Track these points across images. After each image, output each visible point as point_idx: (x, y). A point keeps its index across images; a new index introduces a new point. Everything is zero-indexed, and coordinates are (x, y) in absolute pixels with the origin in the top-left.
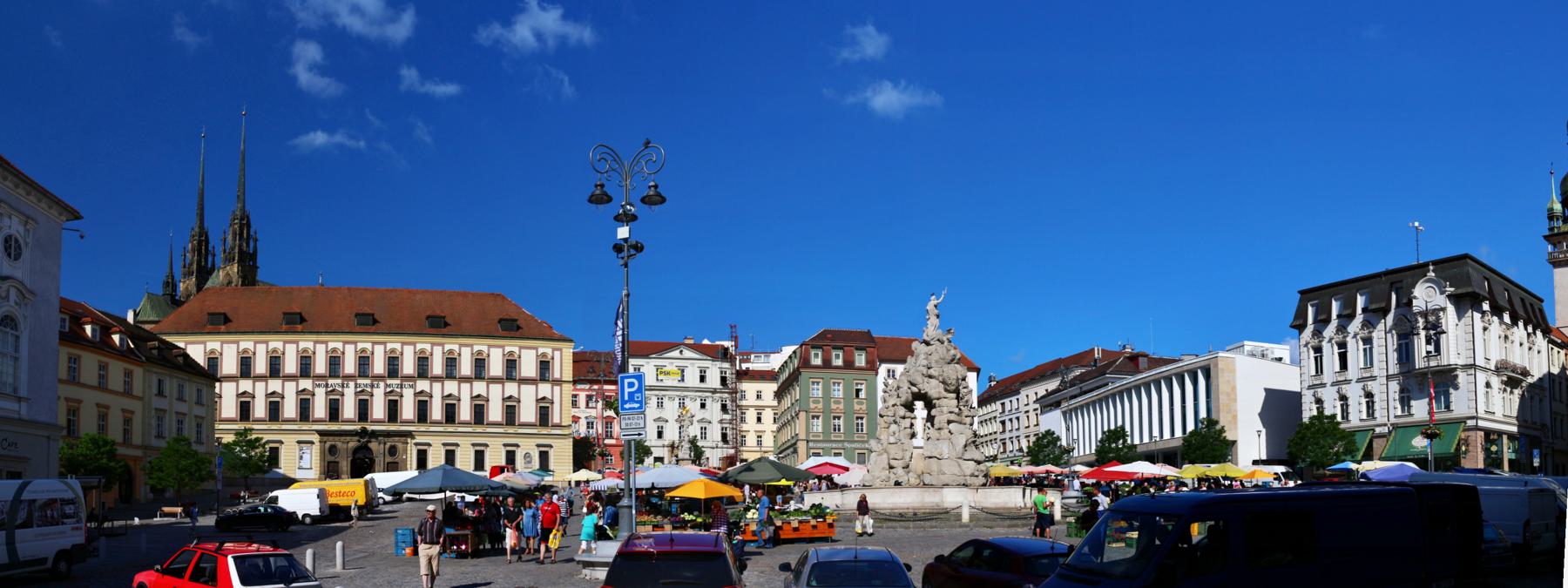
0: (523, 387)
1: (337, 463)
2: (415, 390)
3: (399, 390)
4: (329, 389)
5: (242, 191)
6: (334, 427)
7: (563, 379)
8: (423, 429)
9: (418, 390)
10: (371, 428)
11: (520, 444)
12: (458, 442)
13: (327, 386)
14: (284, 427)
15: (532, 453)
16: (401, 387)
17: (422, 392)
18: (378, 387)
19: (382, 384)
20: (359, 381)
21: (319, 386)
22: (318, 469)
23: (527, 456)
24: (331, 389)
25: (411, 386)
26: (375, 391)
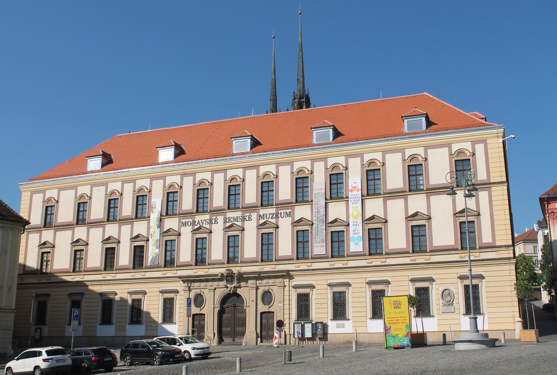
0: (433, 198)
1: (204, 315)
2: (293, 218)
3: (274, 221)
4: (196, 227)
5: (301, 74)
6: (201, 271)
7: (492, 181)
8: (303, 267)
9: (296, 219)
10: (235, 270)
11: (434, 277)
12: (350, 281)
13: (194, 222)
14: (148, 275)
15: (453, 289)
16: (277, 217)
17: (300, 220)
18: (250, 219)
19: (254, 215)
20: (231, 214)
21: (185, 224)
22: (182, 324)
23: (445, 293)
24: (199, 226)
25: (288, 215)
26: (247, 224)
